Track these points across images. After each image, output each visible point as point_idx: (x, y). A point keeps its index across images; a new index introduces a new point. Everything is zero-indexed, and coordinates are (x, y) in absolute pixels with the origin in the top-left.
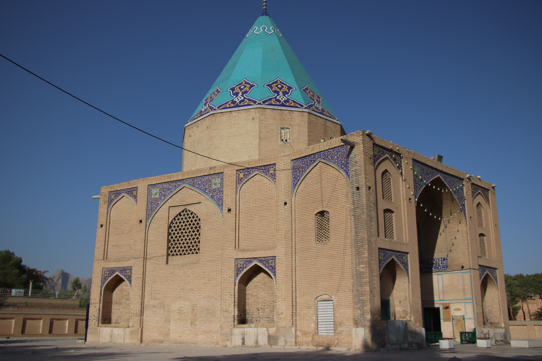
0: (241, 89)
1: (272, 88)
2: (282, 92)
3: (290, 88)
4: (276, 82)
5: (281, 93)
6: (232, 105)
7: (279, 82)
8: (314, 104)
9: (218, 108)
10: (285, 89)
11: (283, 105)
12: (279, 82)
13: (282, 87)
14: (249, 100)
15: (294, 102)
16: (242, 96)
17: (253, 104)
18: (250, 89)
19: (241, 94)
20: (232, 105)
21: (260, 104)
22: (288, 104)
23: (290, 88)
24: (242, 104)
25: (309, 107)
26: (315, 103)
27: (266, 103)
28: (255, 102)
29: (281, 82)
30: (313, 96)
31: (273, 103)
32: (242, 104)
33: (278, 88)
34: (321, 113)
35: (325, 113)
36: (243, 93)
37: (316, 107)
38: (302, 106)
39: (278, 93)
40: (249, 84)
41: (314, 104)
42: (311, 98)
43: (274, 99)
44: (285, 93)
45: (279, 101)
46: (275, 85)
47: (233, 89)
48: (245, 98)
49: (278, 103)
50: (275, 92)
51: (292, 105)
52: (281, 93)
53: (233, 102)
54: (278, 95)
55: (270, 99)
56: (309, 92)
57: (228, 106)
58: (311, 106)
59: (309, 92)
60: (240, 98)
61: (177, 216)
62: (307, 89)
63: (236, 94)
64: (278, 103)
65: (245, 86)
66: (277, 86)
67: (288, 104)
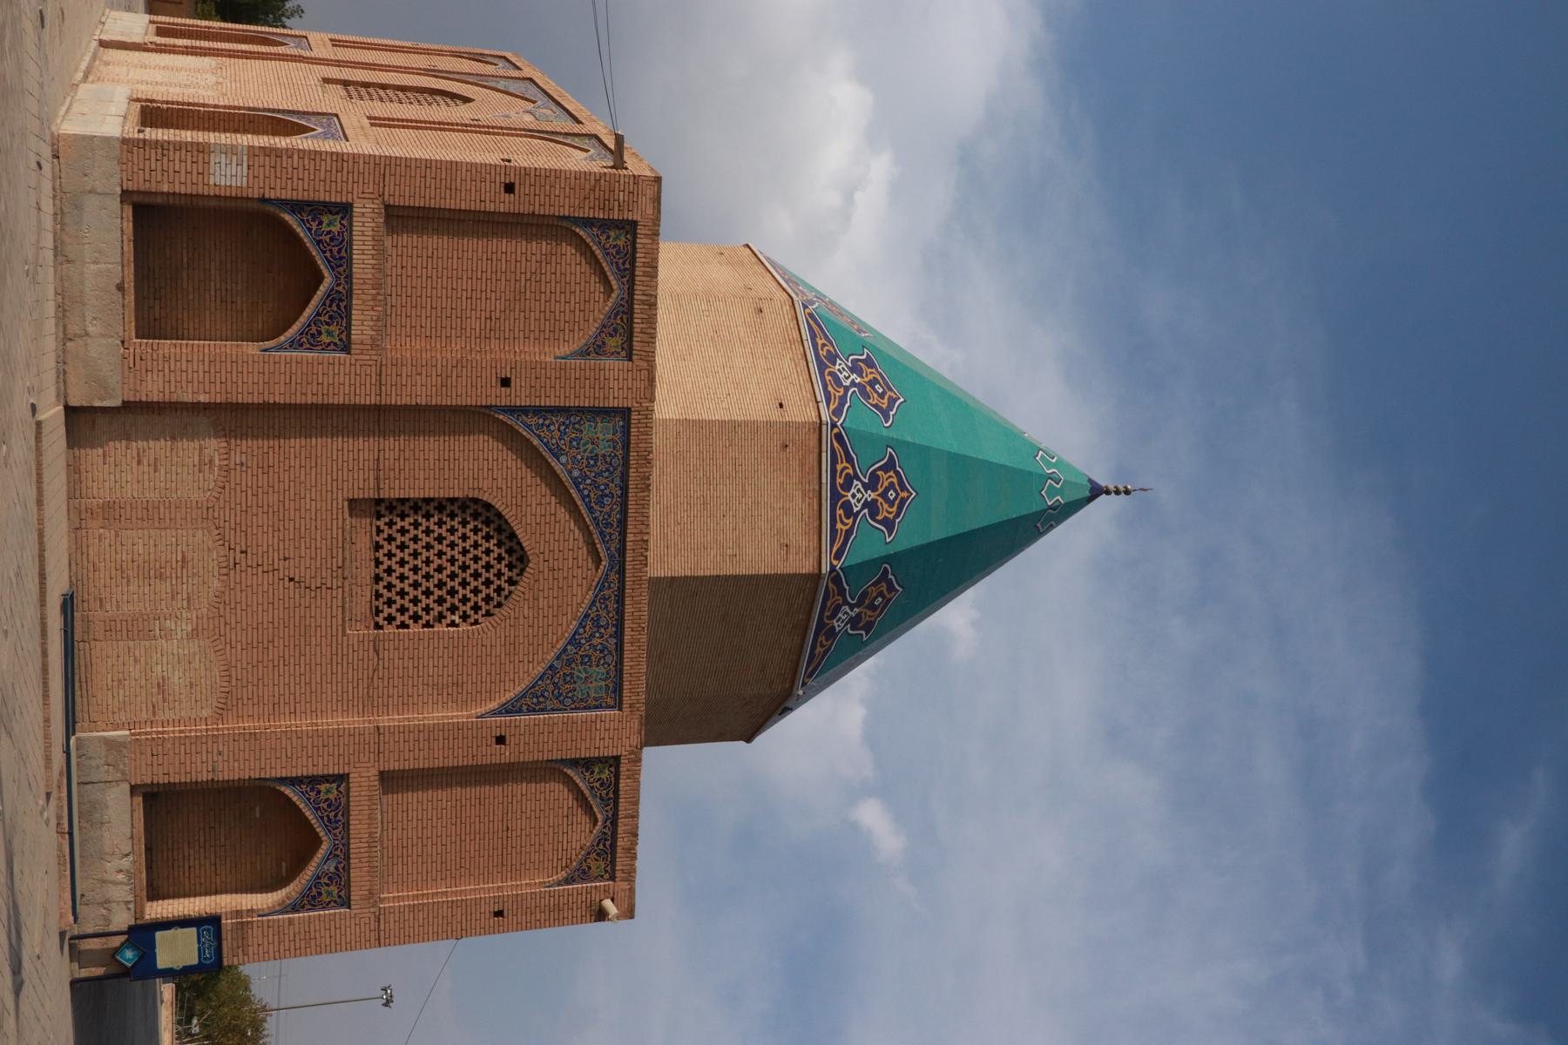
0: (873, 383)
1: (885, 468)
2: (874, 501)
3: (889, 524)
4: (903, 488)
5: (873, 495)
6: (823, 353)
7: (905, 494)
8: (846, 602)
9: (811, 315)
11: (835, 496)
12: (905, 494)
13: (891, 504)
14: (843, 400)
15: (849, 533)
16: (853, 384)
17: (832, 407)
18: (876, 406)
19: (858, 380)
20: (823, 353)
21: (834, 425)
22: (840, 512)
23: (889, 524)
24: (828, 378)
25: (836, 580)
26: (852, 607)
28: (837, 412)
29: (903, 501)
30: (872, 607)
31: (839, 467)
32: (828, 378)
34: (821, 624)
35: (822, 638)
36: (861, 387)
37: (837, 609)
38: (838, 556)
39: (872, 485)
40: (890, 407)
41: (846, 602)
42: (865, 594)
44: (872, 506)
45: (847, 486)
46: (895, 480)
47: (869, 363)
48: (847, 389)
49: (840, 481)
50: (874, 478)
51: (839, 526)
52: (873, 495)
53: (833, 358)
54: (864, 484)
55: (849, 459)
56: (881, 594)
57: (820, 342)
58: (842, 592)
59: (881, 594)
60: (847, 377)
62: (891, 588)
63: (855, 369)
64: (840, 481)
65: (882, 396)
66: (891, 485)
67: (840, 512)
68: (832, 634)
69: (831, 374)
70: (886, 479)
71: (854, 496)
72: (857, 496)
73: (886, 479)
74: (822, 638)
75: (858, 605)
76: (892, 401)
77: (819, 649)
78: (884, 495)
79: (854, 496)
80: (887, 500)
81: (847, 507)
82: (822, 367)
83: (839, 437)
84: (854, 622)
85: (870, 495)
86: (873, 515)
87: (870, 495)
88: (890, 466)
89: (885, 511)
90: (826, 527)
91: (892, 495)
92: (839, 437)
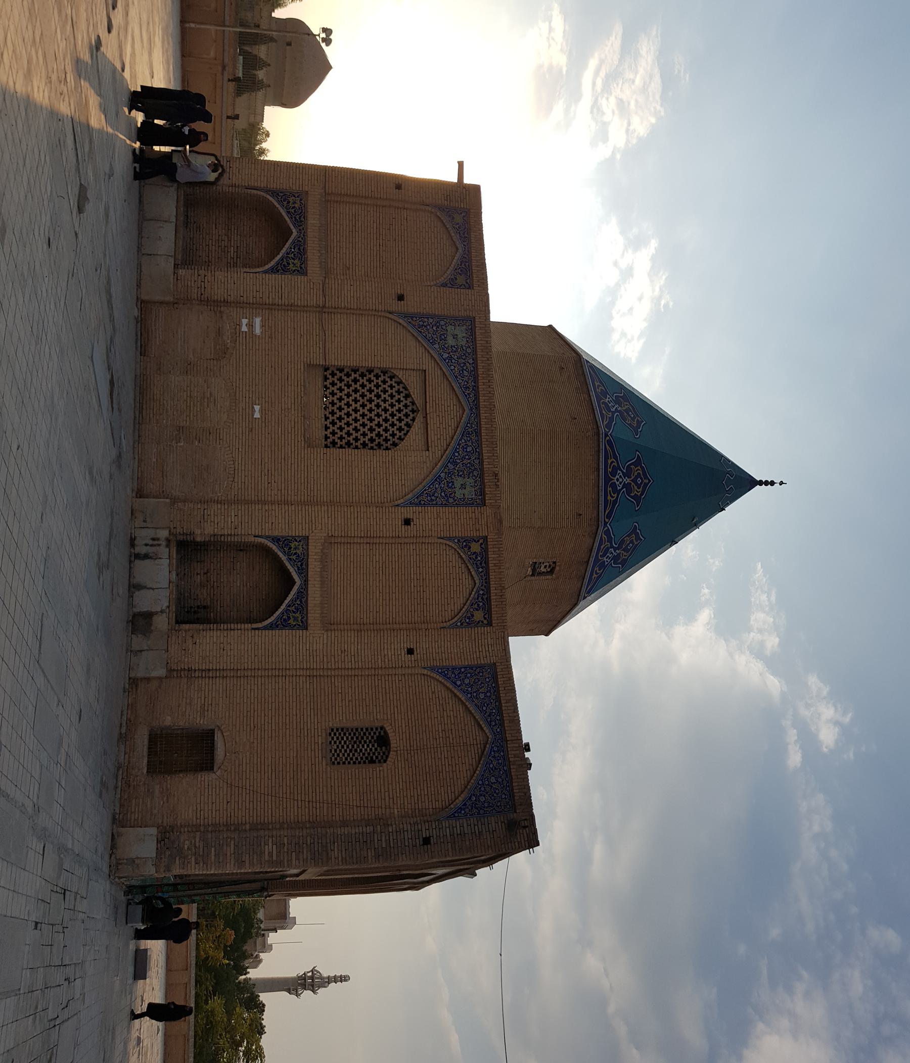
0: (627, 411)
4: (646, 477)
8: (612, 547)
10: (636, 491)
11: (607, 480)
14: (611, 419)
15: (615, 502)
18: (630, 425)
20: (599, 391)
21: (606, 435)
22: (609, 489)
27: (608, 447)
28: (608, 426)
29: (646, 485)
30: (626, 550)
33: (636, 477)
34: (597, 560)
35: (596, 569)
37: (607, 551)
39: (627, 474)
41: (612, 547)
43: (615, 464)
45: (614, 474)
48: (613, 413)
51: (609, 498)
53: (605, 394)
58: (610, 540)
59: (632, 542)
61: (405, 388)
62: (638, 538)
63: (617, 401)
65: (633, 419)
66: (639, 475)
67: (609, 489)
68: (603, 566)
69: (604, 403)
70: (637, 471)
71: (618, 480)
72: (619, 480)
73: (637, 471)
74: (596, 569)
75: (618, 548)
76: (639, 423)
77: (595, 575)
78: (635, 481)
79: (618, 480)
80: (636, 484)
81: (614, 486)
82: (599, 399)
83: (609, 442)
84: (616, 559)
85: (627, 480)
86: (629, 492)
87: (627, 480)
88: (638, 463)
89: (636, 491)
90: (602, 499)
91: (639, 481)
92: (609, 442)
